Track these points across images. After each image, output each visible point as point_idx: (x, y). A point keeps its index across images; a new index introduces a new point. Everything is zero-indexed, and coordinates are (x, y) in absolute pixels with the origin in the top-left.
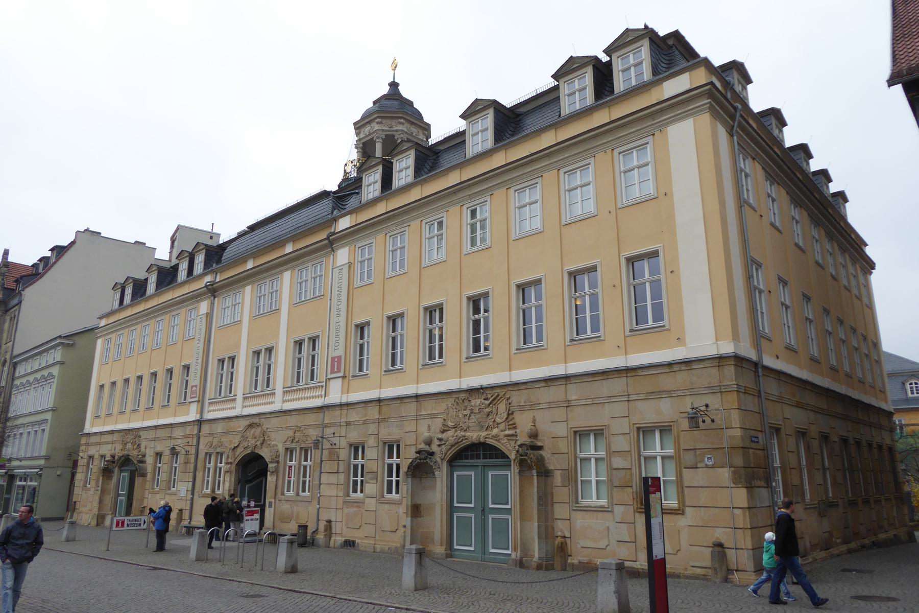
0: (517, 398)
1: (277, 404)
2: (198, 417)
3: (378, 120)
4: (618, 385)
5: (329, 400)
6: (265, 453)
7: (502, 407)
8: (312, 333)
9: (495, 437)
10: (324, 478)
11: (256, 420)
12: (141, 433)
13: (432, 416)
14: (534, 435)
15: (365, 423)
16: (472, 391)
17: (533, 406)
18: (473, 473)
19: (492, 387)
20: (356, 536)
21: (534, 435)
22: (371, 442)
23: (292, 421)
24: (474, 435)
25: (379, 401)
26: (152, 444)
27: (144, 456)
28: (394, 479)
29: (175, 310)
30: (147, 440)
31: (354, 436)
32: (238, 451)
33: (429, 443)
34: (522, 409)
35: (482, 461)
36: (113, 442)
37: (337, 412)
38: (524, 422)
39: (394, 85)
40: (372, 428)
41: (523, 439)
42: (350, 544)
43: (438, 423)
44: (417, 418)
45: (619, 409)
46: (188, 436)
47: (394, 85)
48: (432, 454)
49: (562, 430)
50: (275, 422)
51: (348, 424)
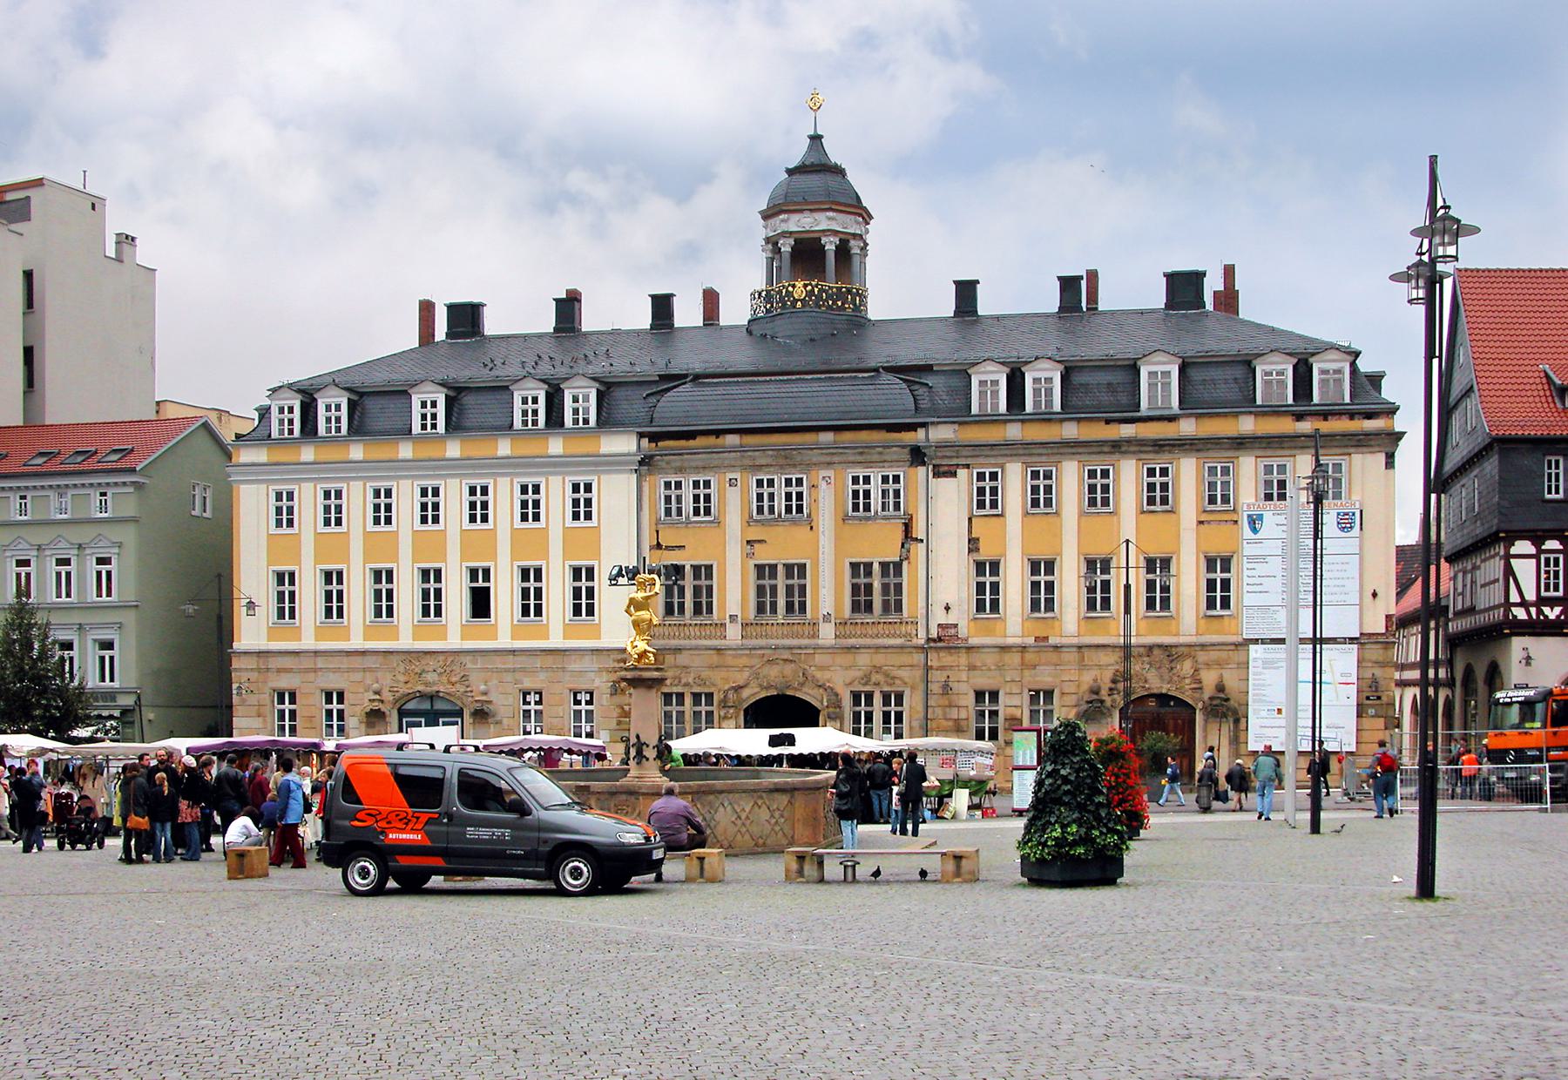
0: (1202, 657)
3: (831, 214)
7: (1186, 667)
14: (1221, 688)
21: (1221, 688)
26: (509, 677)
31: (985, 682)
32: (746, 693)
33: (1096, 692)
34: (1208, 665)
38: (1209, 678)
39: (816, 139)
43: (1108, 675)
44: (1082, 666)
47: (816, 139)
48: (1102, 702)
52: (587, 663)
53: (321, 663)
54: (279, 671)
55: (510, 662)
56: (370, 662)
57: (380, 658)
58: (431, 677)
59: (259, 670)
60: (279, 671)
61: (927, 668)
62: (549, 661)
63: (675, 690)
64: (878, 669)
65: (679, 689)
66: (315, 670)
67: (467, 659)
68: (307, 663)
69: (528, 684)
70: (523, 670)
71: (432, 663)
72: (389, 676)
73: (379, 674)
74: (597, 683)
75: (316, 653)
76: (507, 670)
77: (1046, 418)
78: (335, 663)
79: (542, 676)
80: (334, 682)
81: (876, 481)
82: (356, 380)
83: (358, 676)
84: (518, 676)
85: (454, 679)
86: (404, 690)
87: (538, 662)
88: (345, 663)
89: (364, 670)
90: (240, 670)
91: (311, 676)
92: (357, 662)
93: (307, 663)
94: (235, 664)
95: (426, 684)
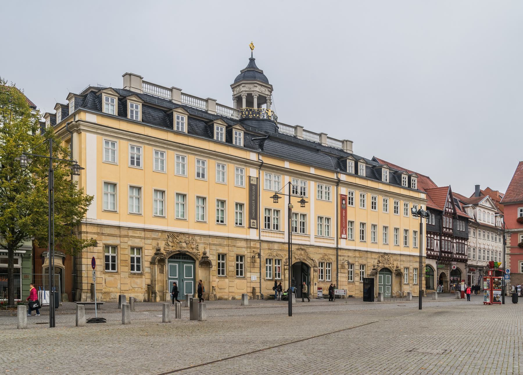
0: (395, 257)
1: (313, 241)
2: (257, 238)
4: (412, 258)
5: (339, 246)
6: (308, 262)
8: (328, 216)
9: (390, 267)
10: (339, 274)
11: (302, 247)
12: (196, 237)
13: (375, 259)
15: (355, 257)
16: (385, 253)
17: (398, 260)
18: (177, 265)
19: (390, 254)
20: (353, 294)
21: (397, 267)
22: (357, 264)
23: (322, 251)
24: (387, 266)
25: (360, 251)
26: (214, 247)
27: (205, 253)
28: (277, 272)
29: (224, 161)
30: (205, 243)
34: (395, 260)
35: (384, 272)
36: (154, 239)
37: (344, 251)
38: (395, 263)
39: (252, 60)
40: (357, 259)
41: (395, 269)
42: (350, 296)
43: (376, 261)
45: (411, 264)
46: (254, 248)
47: (252, 60)
49: (402, 267)
50: (311, 250)
51: (348, 256)
52: (243, 244)
53: (131, 233)
54: (109, 235)
55: (216, 241)
56: (154, 235)
57: (160, 234)
58: (184, 245)
59: (98, 234)
60: (109, 235)
61: (337, 256)
62: (230, 242)
63: (277, 258)
64: (326, 255)
65: (271, 257)
66: (127, 236)
67: (197, 238)
68: (124, 232)
69: (221, 250)
70: (220, 245)
71: (183, 238)
72: (164, 243)
73: (159, 242)
74: (246, 253)
75: (129, 228)
76: (214, 245)
77: (361, 177)
78: (138, 234)
79: (227, 248)
80: (137, 243)
81: (324, 187)
82: (148, 99)
83: (149, 241)
84: (218, 247)
85: (193, 246)
86: (171, 249)
87: (226, 242)
88: (142, 234)
89: (154, 239)
90: (87, 233)
91: (126, 239)
92: (148, 235)
93: (124, 232)
94: (84, 228)
95: (181, 248)
